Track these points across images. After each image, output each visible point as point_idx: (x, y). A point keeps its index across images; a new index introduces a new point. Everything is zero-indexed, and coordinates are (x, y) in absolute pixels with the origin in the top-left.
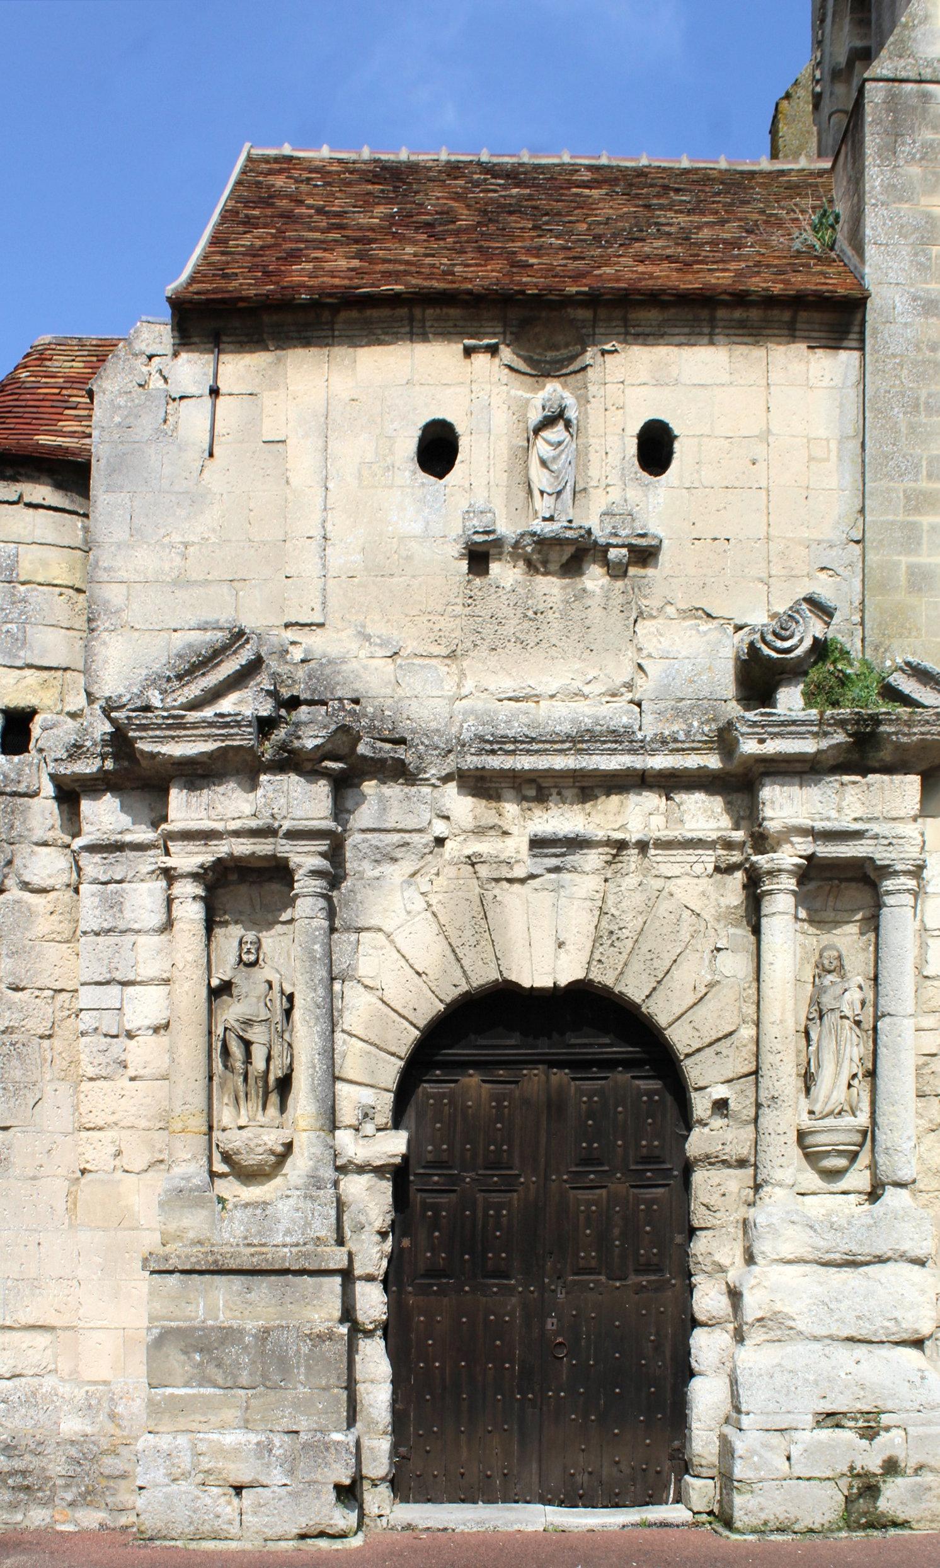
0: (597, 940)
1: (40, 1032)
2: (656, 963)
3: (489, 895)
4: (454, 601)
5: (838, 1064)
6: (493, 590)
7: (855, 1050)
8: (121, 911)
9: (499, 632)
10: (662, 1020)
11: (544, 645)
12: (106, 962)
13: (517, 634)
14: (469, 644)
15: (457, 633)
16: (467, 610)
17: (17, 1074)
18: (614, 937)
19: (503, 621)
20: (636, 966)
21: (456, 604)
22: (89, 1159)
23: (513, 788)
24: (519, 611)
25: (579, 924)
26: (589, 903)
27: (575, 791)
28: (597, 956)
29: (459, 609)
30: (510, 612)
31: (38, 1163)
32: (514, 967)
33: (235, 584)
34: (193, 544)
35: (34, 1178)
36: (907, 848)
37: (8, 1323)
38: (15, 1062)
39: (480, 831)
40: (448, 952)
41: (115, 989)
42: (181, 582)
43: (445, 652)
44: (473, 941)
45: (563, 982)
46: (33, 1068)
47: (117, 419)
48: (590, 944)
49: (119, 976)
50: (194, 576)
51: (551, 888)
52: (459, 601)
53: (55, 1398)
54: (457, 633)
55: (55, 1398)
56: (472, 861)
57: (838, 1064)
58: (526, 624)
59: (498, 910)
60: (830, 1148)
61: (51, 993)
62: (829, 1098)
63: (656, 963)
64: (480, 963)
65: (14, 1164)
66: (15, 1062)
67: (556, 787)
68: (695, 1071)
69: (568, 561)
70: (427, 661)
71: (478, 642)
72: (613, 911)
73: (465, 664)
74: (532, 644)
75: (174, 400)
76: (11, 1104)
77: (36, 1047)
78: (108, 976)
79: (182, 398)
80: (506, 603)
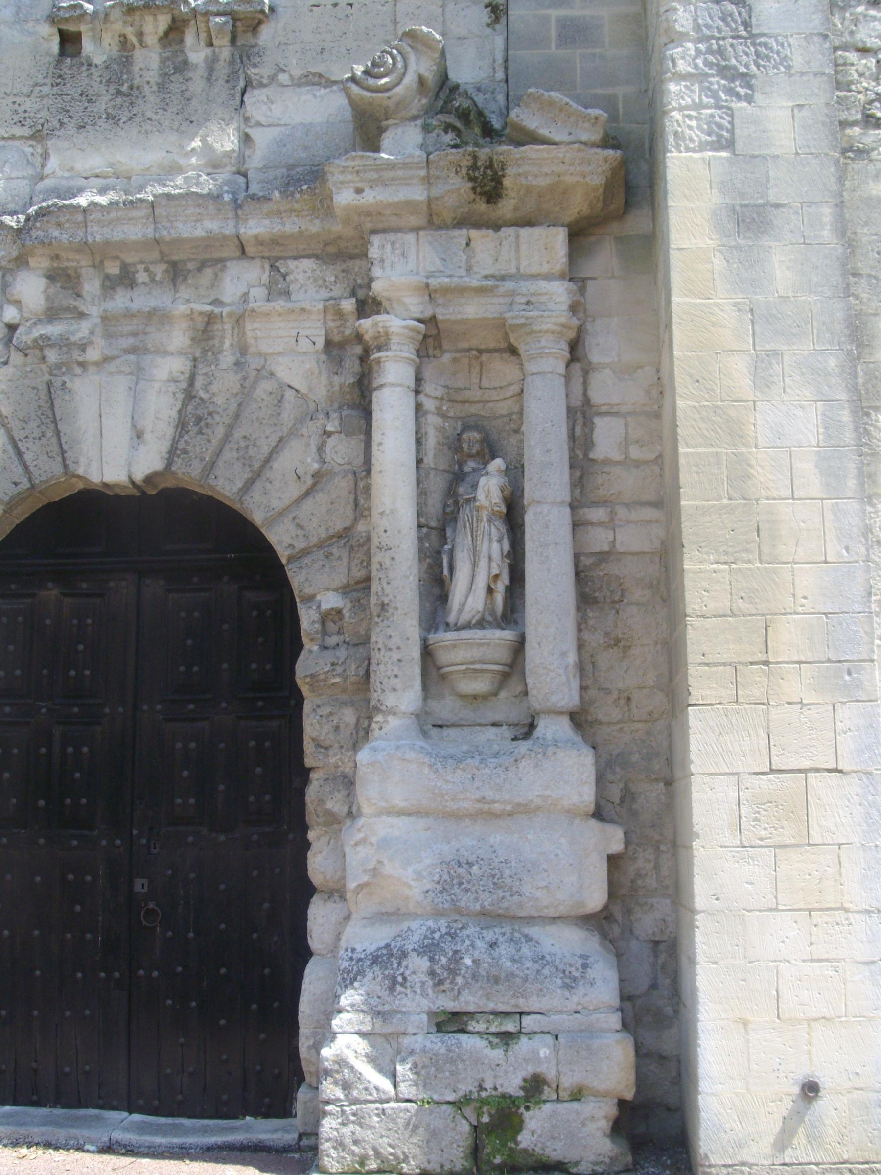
0: (182, 425)
2: (252, 452)
3: (57, 382)
4: (41, 81)
5: (474, 565)
6: (84, 68)
7: (493, 546)
9: (89, 109)
10: (258, 518)
11: (137, 119)
13: (110, 111)
14: (56, 123)
15: (44, 113)
16: (55, 90)
18: (202, 424)
19: (94, 98)
20: (228, 455)
21: (45, 84)
23: (94, 266)
24: (112, 90)
25: (161, 409)
26: (172, 387)
27: (164, 267)
28: (181, 445)
29: (46, 89)
30: (103, 89)
32: (82, 460)
36: (551, 305)
39: (52, 314)
40: (10, 448)
43: (27, 132)
44: (37, 433)
45: (139, 476)
48: (170, 431)
51: (128, 370)
52: (49, 81)
54: (44, 113)
56: (41, 344)
57: (474, 565)
58: (119, 100)
59: (67, 398)
60: (464, 667)
62: (463, 605)
63: (252, 452)
64: (46, 457)
67: (142, 262)
68: (297, 579)
69: (167, 34)
70: (10, 143)
71: (66, 120)
72: (202, 394)
73: (49, 143)
74: (125, 119)
80: (99, 80)
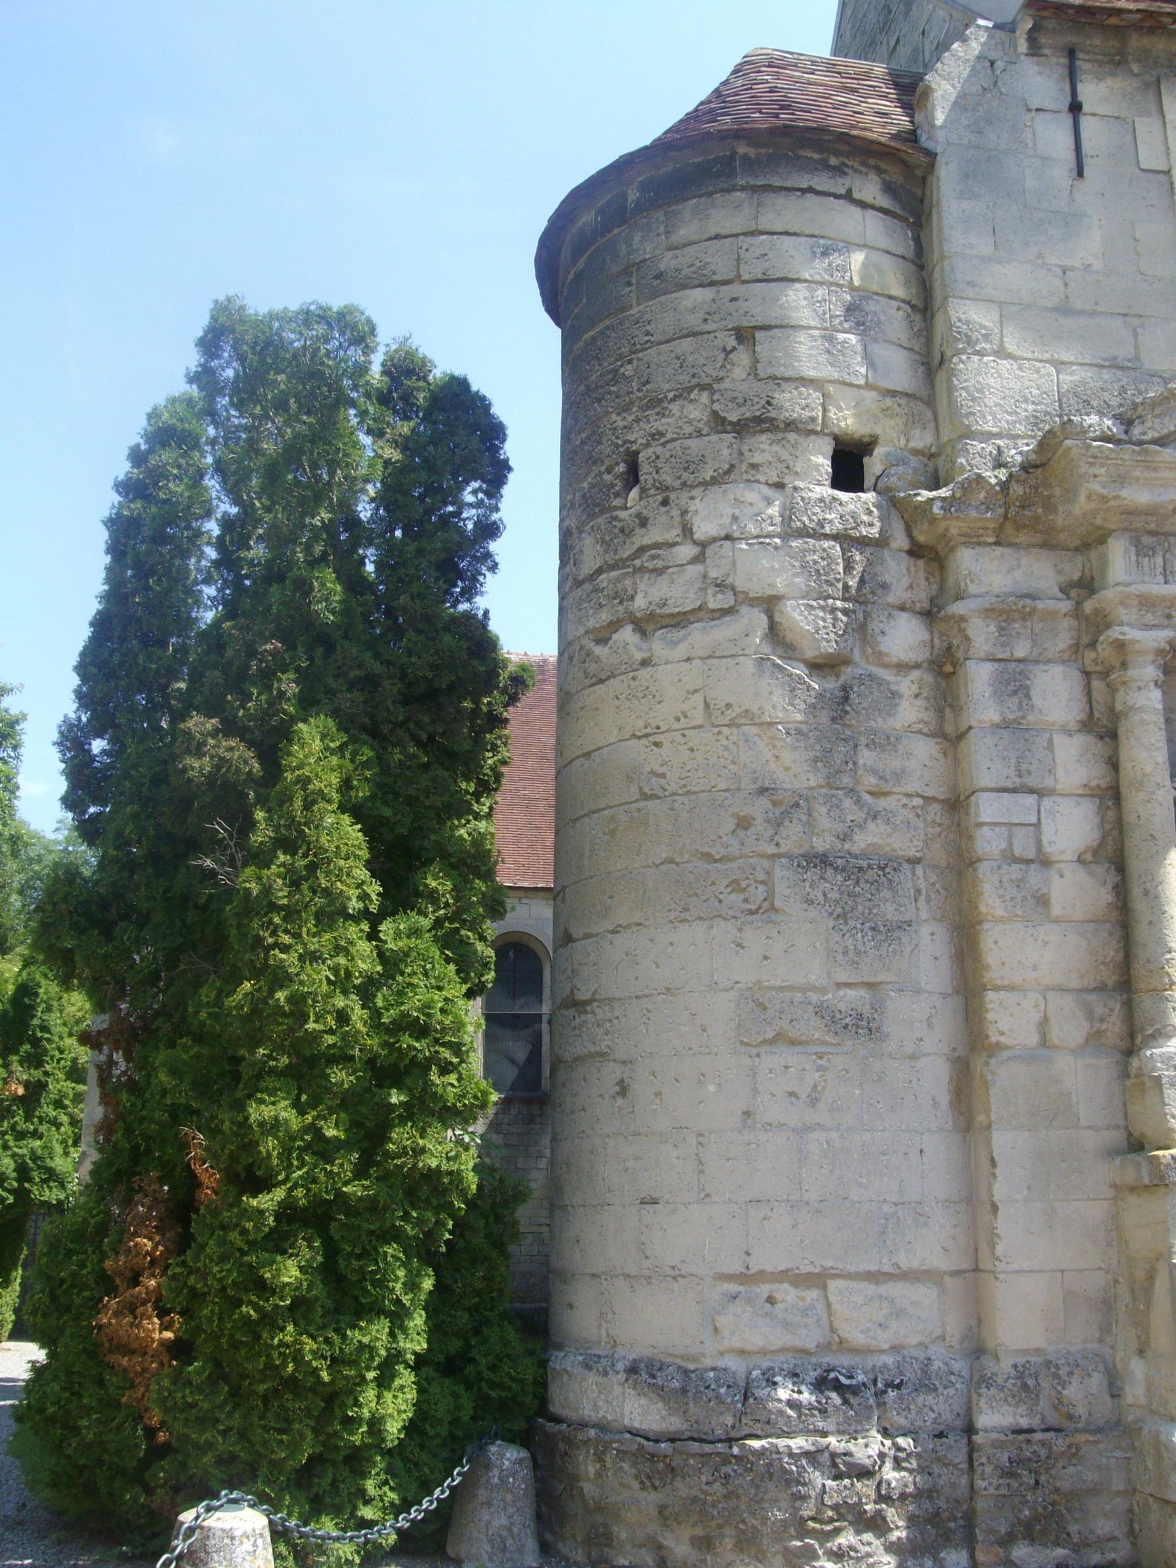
1: (912, 853)
8: (1028, 696)
12: (1013, 761)
17: (889, 910)
22: (1005, 1029)
31: (918, 1035)
33: (1128, 319)
34: (1073, 269)
35: (913, 1057)
37: (886, 1268)
38: (886, 893)
41: (1030, 800)
42: (1064, 310)
46: (906, 901)
47: (964, 122)
49: (1032, 781)
50: (1079, 305)
53: (953, 1378)
55: (953, 1378)
61: (920, 801)
65: (888, 1035)
66: (886, 893)
75: (1029, 110)
76: (883, 951)
77: (909, 873)
78: (1018, 781)
79: (1037, 110)
